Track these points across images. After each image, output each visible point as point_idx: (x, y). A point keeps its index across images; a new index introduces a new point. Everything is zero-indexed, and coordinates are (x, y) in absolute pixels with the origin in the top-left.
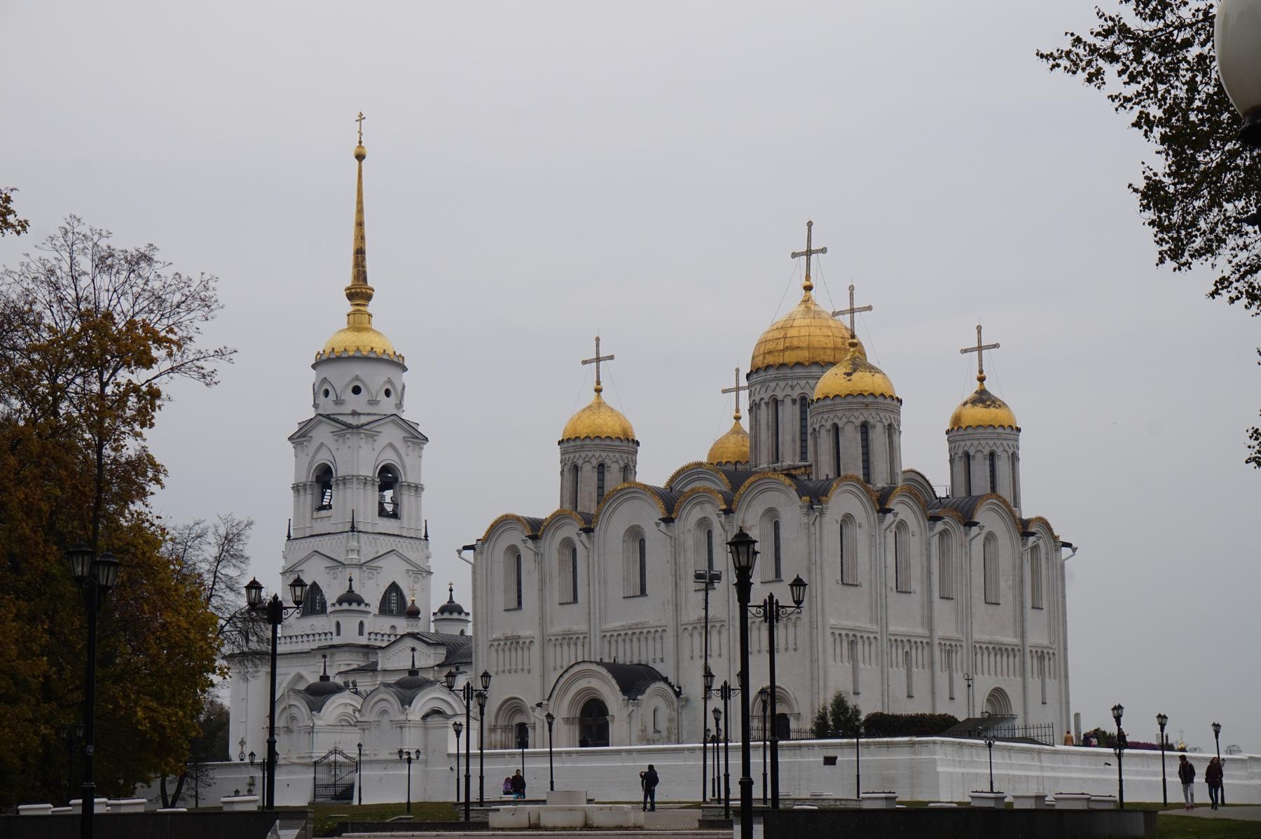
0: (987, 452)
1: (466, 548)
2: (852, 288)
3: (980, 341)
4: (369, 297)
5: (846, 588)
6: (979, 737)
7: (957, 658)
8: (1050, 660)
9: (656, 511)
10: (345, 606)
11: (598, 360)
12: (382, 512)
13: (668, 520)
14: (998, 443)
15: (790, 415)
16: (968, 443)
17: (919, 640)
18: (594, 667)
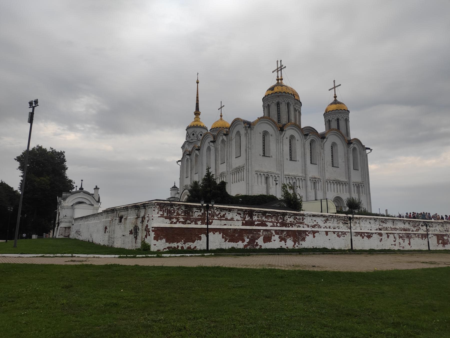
0: (336, 118)
3: (334, 85)
4: (199, 114)
5: (264, 157)
7: (319, 186)
13: (213, 142)
14: (340, 115)
16: (329, 117)
17: (300, 178)
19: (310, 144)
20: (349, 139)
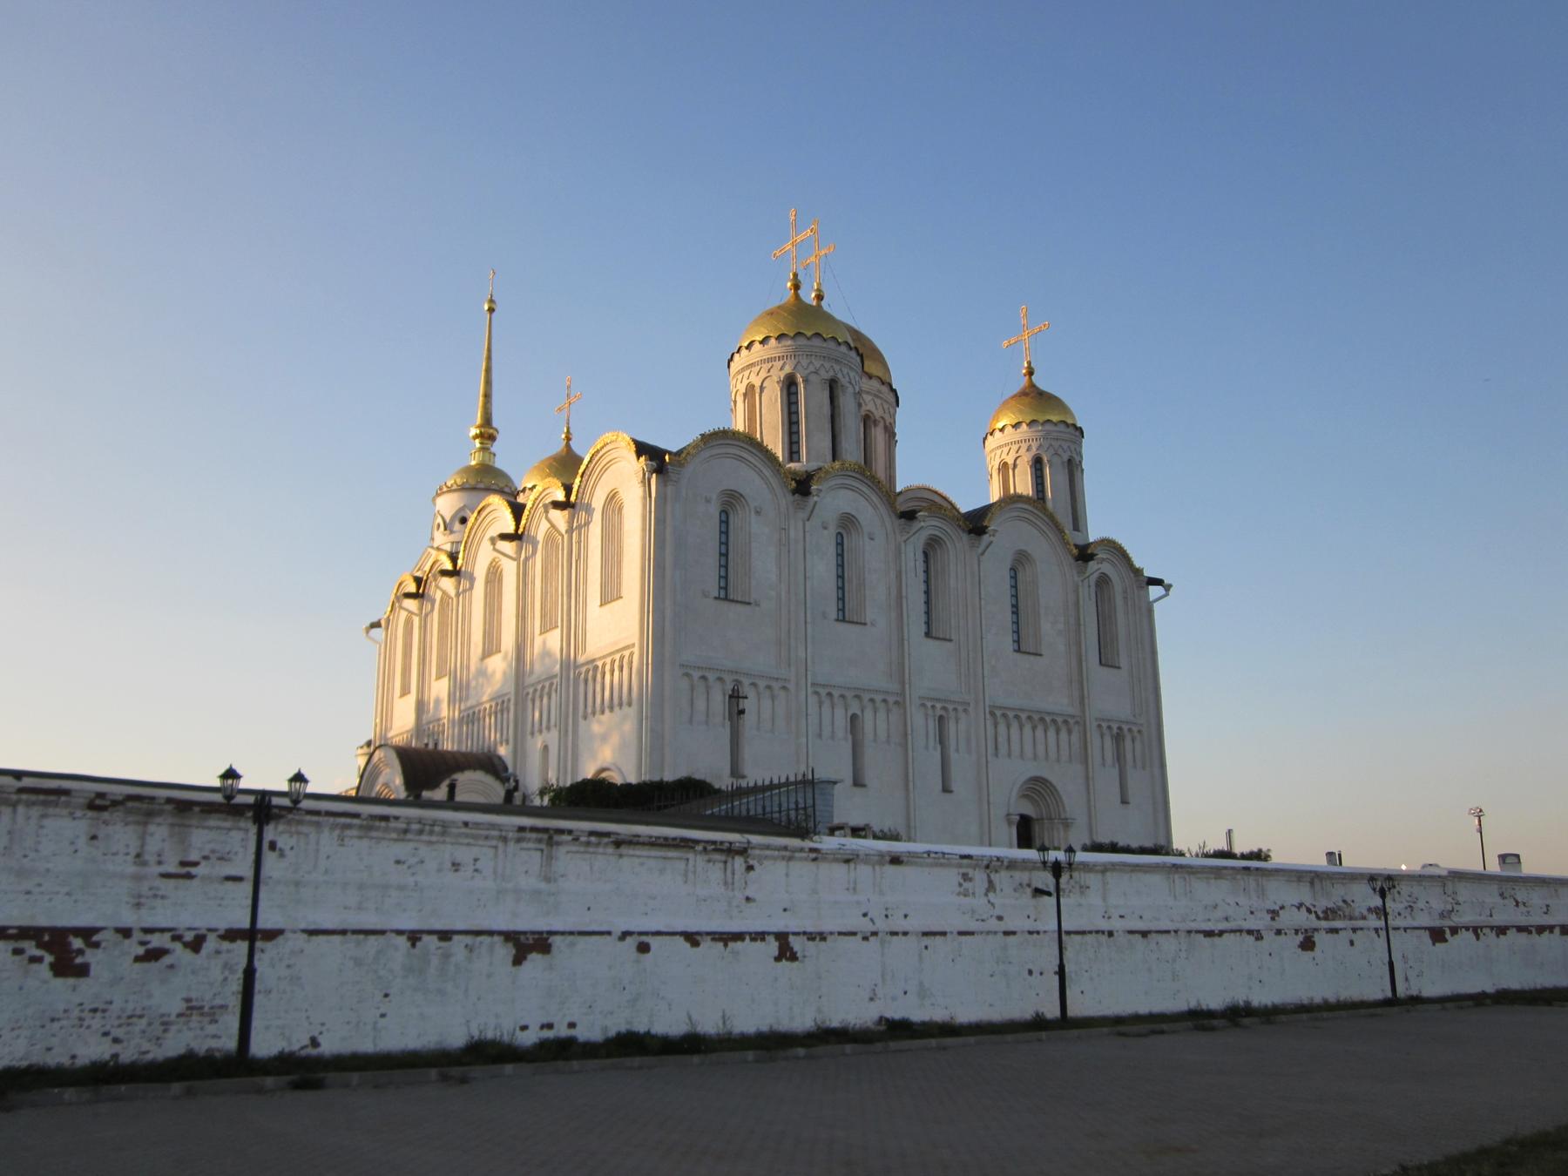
4: (492, 438)
5: (725, 605)
19: (926, 554)
20: (1081, 542)
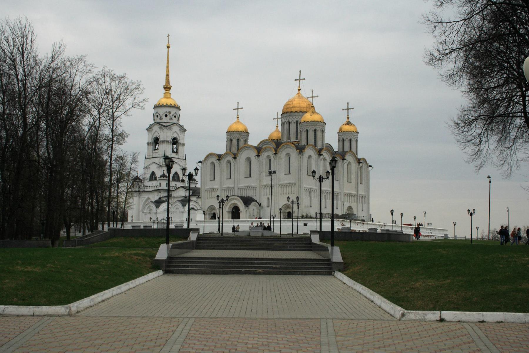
0: (349, 139)
1: (200, 162)
2: (313, 91)
4: (170, 88)
6: (347, 219)
8: (364, 199)
9: (255, 153)
10: (162, 178)
11: (238, 109)
12: (173, 151)
13: (258, 156)
15: (293, 127)
18: (236, 197)
